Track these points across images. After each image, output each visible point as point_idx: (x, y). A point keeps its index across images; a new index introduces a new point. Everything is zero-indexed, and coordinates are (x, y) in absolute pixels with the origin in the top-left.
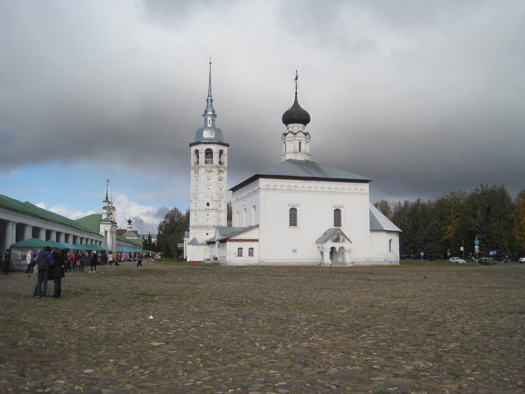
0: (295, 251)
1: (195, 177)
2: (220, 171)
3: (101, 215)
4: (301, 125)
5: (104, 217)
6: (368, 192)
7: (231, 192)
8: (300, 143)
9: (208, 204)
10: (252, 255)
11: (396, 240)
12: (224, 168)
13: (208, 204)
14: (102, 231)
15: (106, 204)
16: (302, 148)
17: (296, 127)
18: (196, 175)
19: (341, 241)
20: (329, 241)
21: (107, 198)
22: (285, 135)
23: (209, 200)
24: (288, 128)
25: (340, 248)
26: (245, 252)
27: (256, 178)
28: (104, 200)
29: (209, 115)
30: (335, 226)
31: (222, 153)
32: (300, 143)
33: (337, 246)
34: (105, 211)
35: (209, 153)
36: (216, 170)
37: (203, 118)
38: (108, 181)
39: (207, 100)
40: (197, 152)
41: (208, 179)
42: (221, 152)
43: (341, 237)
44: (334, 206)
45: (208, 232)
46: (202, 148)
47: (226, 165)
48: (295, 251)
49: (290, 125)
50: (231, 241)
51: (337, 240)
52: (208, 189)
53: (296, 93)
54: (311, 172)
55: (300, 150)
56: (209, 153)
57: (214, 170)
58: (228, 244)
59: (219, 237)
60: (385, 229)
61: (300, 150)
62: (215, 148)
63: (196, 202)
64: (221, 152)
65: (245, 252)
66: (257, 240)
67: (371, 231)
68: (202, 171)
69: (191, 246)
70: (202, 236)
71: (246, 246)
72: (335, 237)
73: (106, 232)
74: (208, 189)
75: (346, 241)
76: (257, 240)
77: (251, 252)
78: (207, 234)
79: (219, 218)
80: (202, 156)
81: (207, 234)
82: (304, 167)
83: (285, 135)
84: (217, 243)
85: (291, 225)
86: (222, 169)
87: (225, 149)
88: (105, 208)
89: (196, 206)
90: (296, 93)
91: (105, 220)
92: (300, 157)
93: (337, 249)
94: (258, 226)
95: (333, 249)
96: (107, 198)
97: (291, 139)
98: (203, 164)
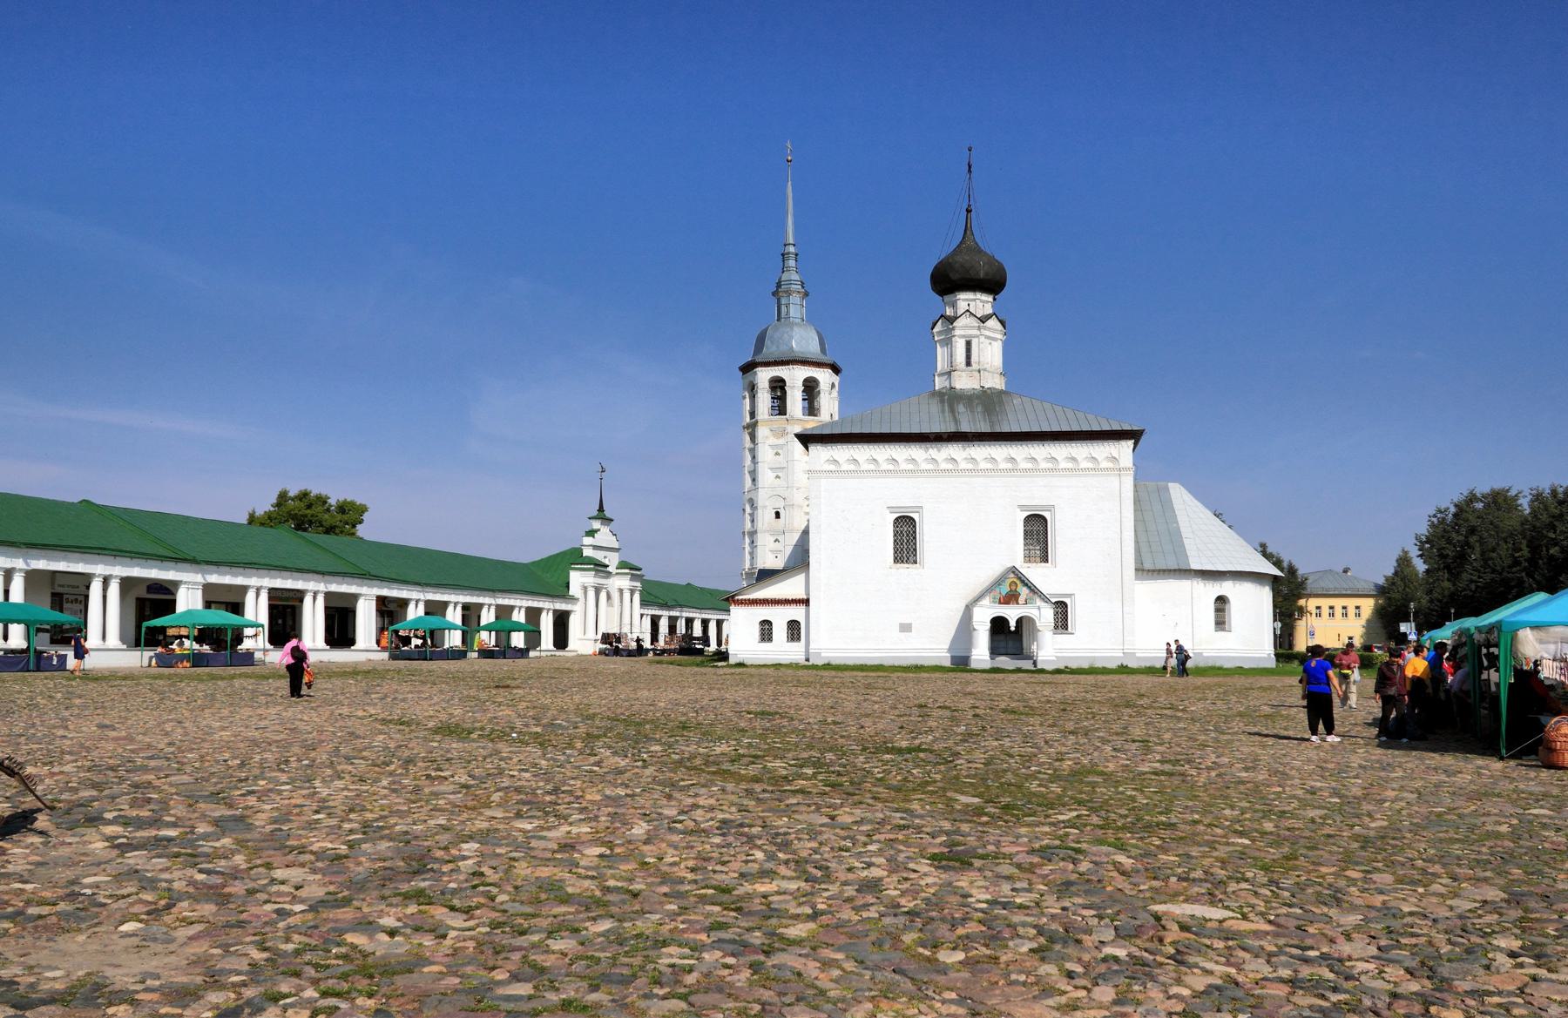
0: (906, 628)
4: (990, 298)
8: (968, 344)
9: (778, 515)
10: (770, 640)
13: (778, 515)
14: (575, 589)
16: (974, 358)
17: (967, 301)
19: (1021, 600)
20: (986, 601)
21: (601, 509)
23: (780, 504)
25: (1019, 621)
26: (780, 631)
28: (595, 513)
32: (968, 344)
33: (1012, 614)
35: (778, 386)
42: (810, 387)
43: (1024, 591)
46: (764, 376)
48: (906, 628)
49: (947, 298)
50: (742, 602)
51: (1011, 598)
53: (969, 211)
55: (968, 363)
60: (1194, 566)
61: (968, 363)
64: (810, 387)
65: (780, 631)
67: (1143, 572)
68: (762, 432)
71: (780, 617)
72: (1005, 589)
73: (585, 589)
75: (1039, 602)
80: (764, 399)
85: (896, 560)
87: (824, 377)
95: (998, 625)
96: (601, 509)
98: (767, 417)
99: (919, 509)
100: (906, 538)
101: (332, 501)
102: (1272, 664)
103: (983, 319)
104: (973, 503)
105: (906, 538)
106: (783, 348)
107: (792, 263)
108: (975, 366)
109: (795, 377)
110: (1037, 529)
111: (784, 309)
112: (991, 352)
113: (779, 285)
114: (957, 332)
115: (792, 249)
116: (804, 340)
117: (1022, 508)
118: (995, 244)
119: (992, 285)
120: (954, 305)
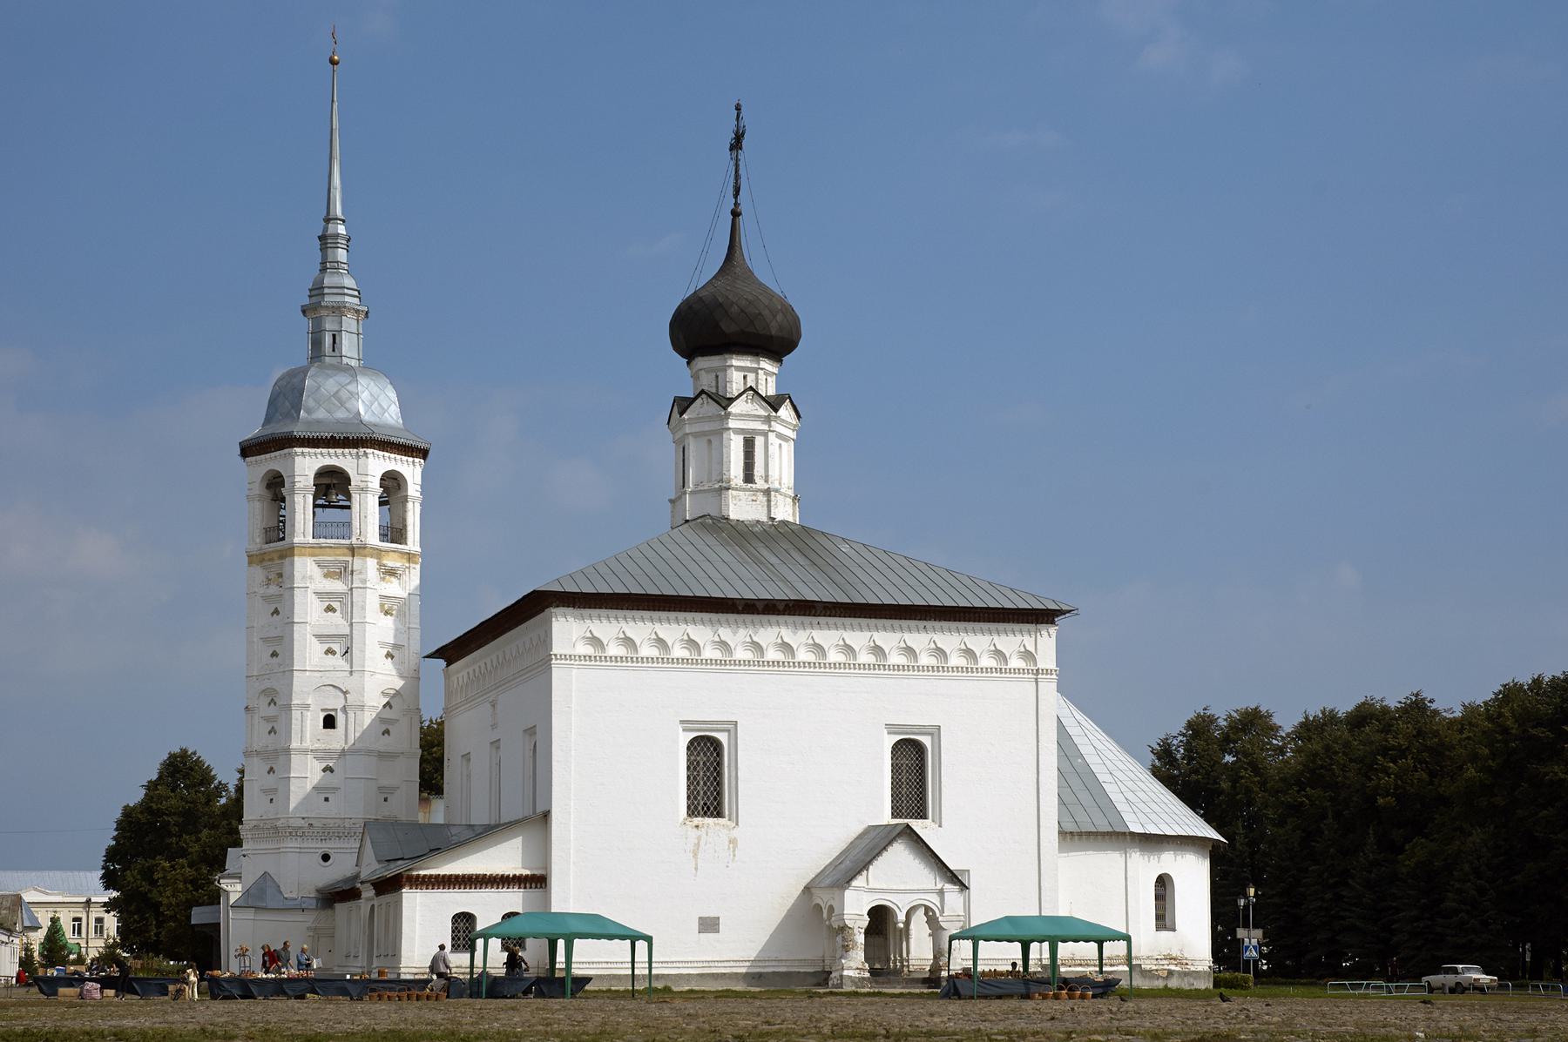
0: (709, 925)
1: (266, 598)
2: (392, 572)
6: (1052, 665)
7: (442, 663)
8: (749, 445)
11: (1193, 879)
13: (329, 722)
16: (758, 470)
18: (273, 589)
22: (683, 404)
23: (335, 702)
24: (696, 377)
27: (535, 605)
30: (894, 816)
32: (749, 445)
35: (332, 486)
37: (306, 324)
42: (392, 484)
44: (892, 728)
45: (326, 847)
46: (306, 465)
47: (413, 543)
48: (709, 925)
49: (702, 362)
53: (736, 214)
54: (791, 577)
55: (749, 477)
57: (357, 563)
58: (413, 900)
59: (371, 868)
61: (749, 477)
63: (272, 711)
64: (392, 484)
69: (249, 914)
70: (302, 873)
71: (489, 907)
78: (326, 858)
79: (385, 782)
81: (326, 858)
82: (765, 553)
83: (683, 404)
84: (368, 892)
85: (692, 811)
86: (390, 562)
87: (411, 471)
89: (272, 731)
90: (736, 214)
92: (742, 508)
93: (901, 917)
97: (707, 427)
99: (732, 727)
100: (708, 778)
101: (1287, 720)
102: (1206, 984)
103: (774, 404)
104: (815, 719)
105: (708, 778)
106: (341, 414)
107: (342, 255)
108: (760, 484)
109: (369, 468)
110: (912, 765)
111: (328, 339)
112: (779, 462)
113: (318, 290)
114: (732, 424)
115: (342, 229)
116: (376, 402)
117: (892, 728)
118: (776, 270)
119: (773, 341)
120: (720, 375)
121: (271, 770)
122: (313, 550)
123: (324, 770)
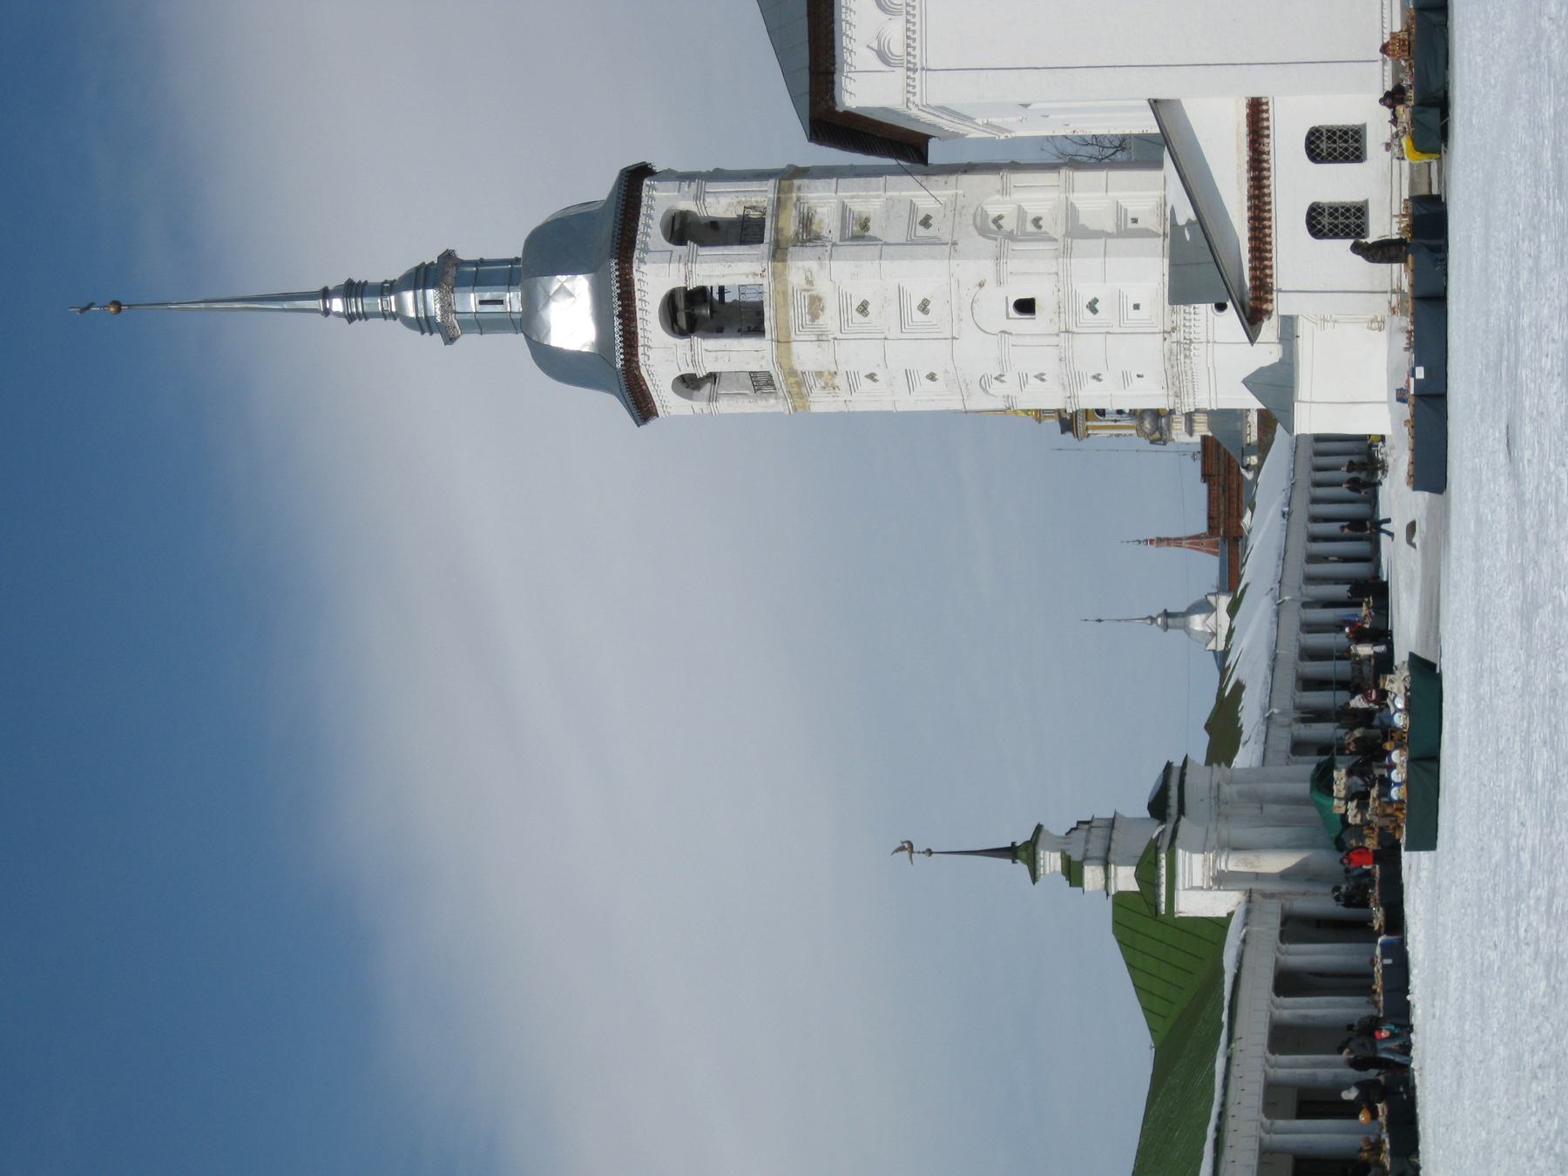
1: (852, 388)
3: (1121, 900)
5: (1125, 879)
9: (1026, 306)
12: (779, 204)
13: (1026, 306)
15: (1051, 862)
18: (840, 381)
21: (1011, 852)
28: (1021, 868)
29: (447, 308)
31: (684, 215)
34: (1092, 875)
36: (800, 268)
38: (907, 847)
39: (351, 318)
40: (688, 383)
41: (863, 309)
42: (683, 230)
46: (663, 356)
52: (924, 307)
56: (694, 312)
62: (658, 276)
64: (683, 230)
66: (1256, 110)
68: (806, 355)
71: (1299, 184)
73: (1222, 880)
74: (924, 307)
76: (1256, 110)
77: (1338, 145)
79: (1110, 226)
86: (791, 225)
87: (660, 201)
88: (1072, 872)
89: (1041, 377)
91: (1147, 870)
94: (1155, 104)
96: (1011, 852)
121: (1097, 378)
122: (783, 342)
123: (1094, 311)
